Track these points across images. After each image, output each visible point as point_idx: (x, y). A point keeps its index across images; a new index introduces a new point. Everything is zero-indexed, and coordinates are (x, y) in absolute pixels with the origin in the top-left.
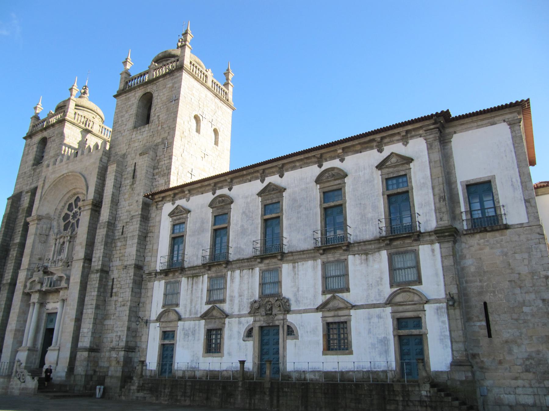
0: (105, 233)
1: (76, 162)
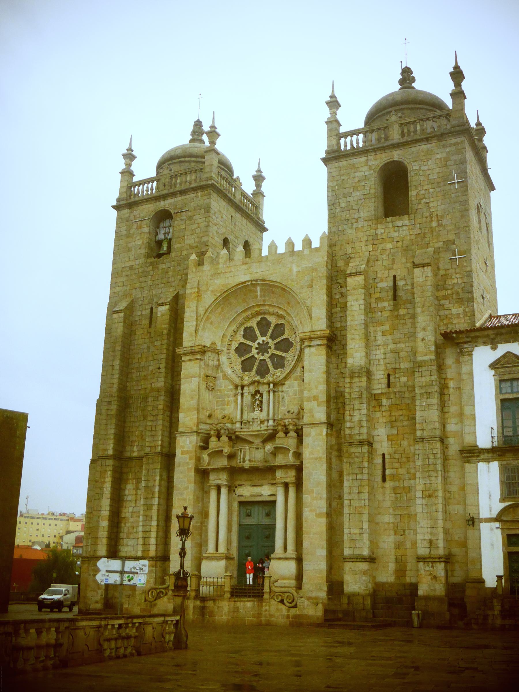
0: (364, 384)
1: (268, 264)
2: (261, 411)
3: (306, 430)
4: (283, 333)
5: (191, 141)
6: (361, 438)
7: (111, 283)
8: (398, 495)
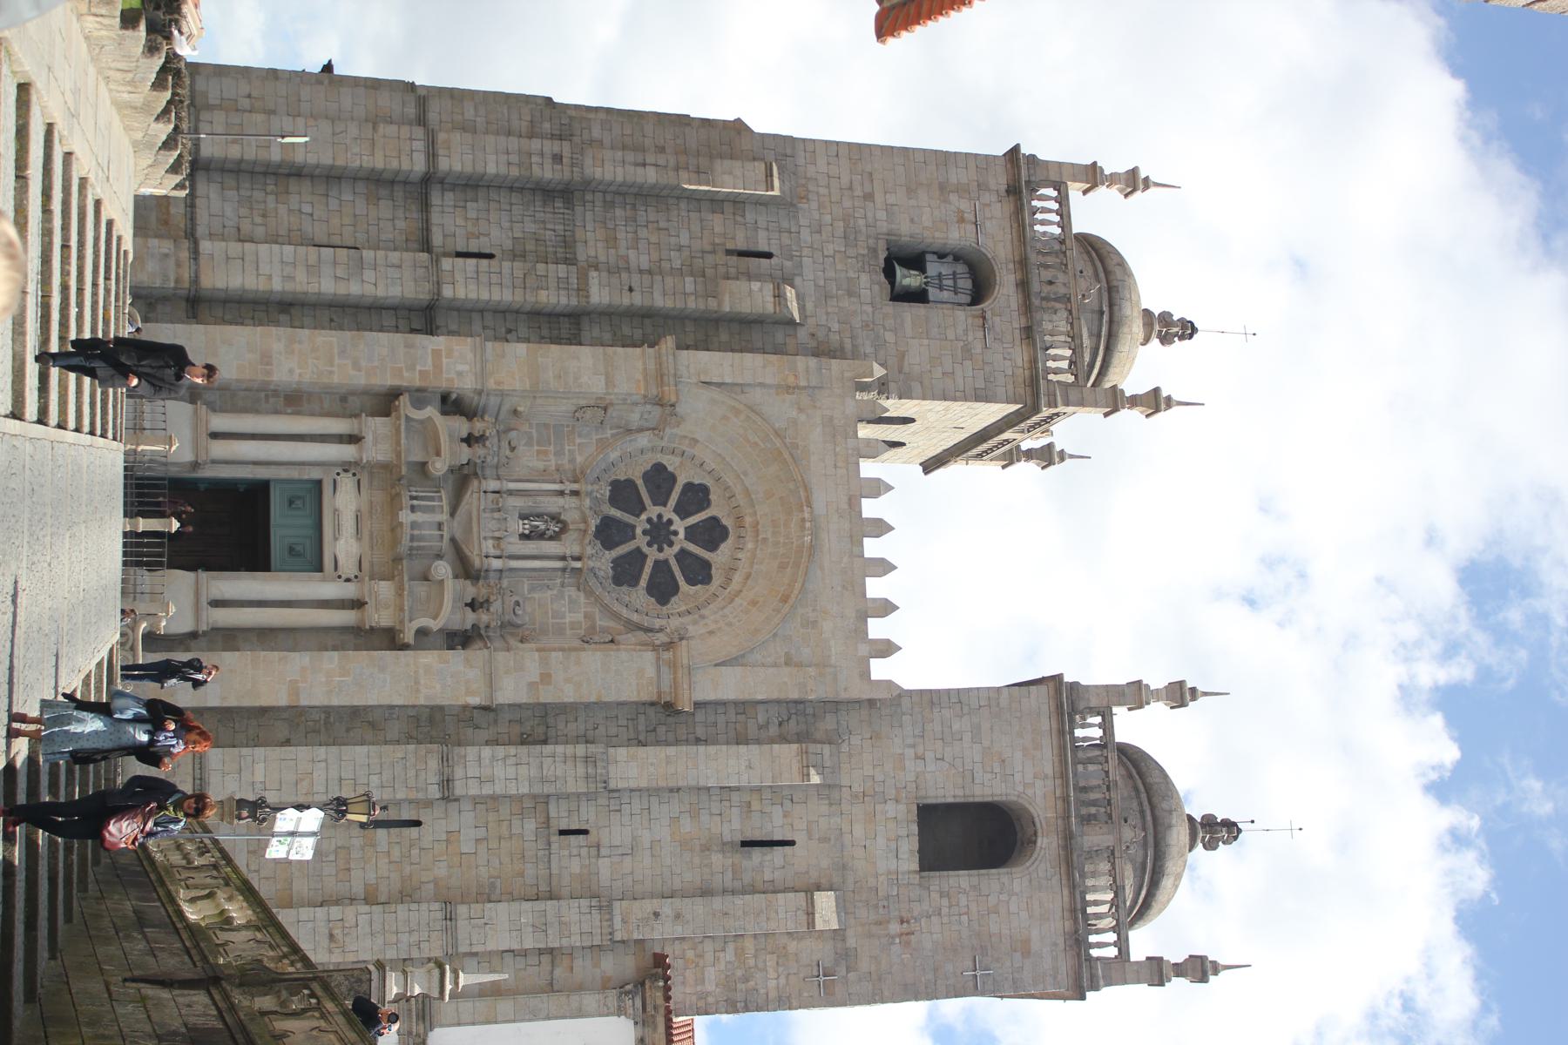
0: (571, 788)
1: (845, 559)
2: (524, 537)
3: (477, 654)
4: (692, 582)
5: (1147, 313)
6: (457, 783)
7: (837, 143)
8: (332, 858)
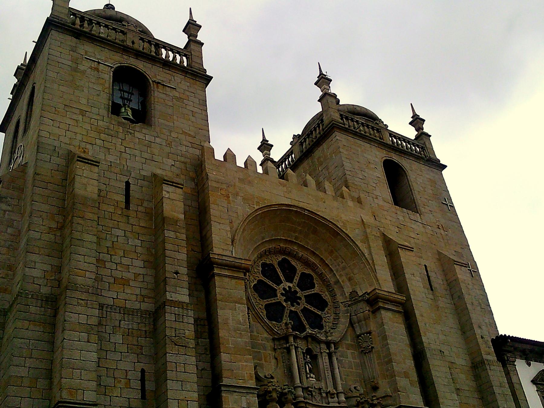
4: (313, 286)
